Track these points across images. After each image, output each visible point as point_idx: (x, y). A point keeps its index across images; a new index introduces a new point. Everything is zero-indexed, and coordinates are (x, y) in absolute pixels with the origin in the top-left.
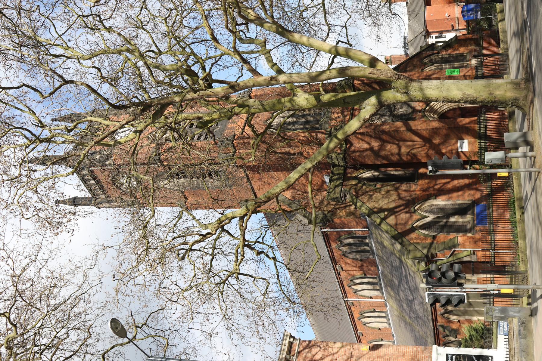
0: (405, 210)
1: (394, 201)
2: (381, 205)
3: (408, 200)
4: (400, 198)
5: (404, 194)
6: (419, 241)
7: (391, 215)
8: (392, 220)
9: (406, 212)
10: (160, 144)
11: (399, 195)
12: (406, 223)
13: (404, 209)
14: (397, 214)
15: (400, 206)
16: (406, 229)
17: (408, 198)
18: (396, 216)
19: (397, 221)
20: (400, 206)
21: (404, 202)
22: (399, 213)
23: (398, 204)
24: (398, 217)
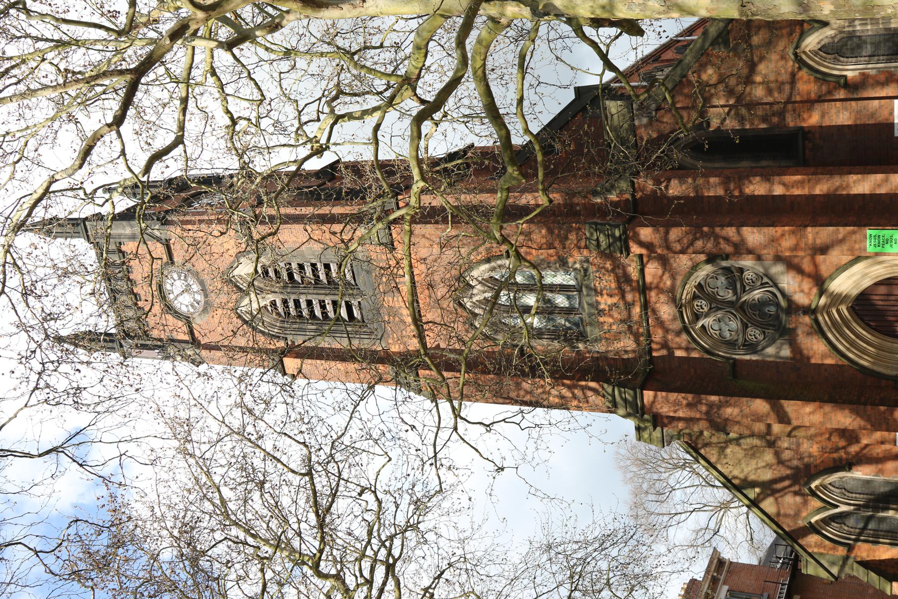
0: (792, 489)
1: (769, 466)
2: (746, 470)
3: (796, 468)
4: (780, 462)
5: (787, 455)
6: (822, 550)
7: (769, 495)
8: (621, 11)
9: (796, 493)
10: (304, 270)
11: (777, 454)
12: (797, 515)
13: (790, 486)
14: (777, 495)
15: (781, 479)
16: (798, 526)
17: (795, 463)
18: (776, 499)
19: (779, 508)
20: (781, 479)
21: (788, 472)
22: (782, 493)
23: (777, 474)
24: (780, 499)
